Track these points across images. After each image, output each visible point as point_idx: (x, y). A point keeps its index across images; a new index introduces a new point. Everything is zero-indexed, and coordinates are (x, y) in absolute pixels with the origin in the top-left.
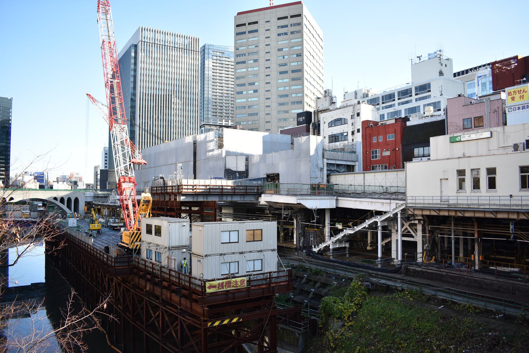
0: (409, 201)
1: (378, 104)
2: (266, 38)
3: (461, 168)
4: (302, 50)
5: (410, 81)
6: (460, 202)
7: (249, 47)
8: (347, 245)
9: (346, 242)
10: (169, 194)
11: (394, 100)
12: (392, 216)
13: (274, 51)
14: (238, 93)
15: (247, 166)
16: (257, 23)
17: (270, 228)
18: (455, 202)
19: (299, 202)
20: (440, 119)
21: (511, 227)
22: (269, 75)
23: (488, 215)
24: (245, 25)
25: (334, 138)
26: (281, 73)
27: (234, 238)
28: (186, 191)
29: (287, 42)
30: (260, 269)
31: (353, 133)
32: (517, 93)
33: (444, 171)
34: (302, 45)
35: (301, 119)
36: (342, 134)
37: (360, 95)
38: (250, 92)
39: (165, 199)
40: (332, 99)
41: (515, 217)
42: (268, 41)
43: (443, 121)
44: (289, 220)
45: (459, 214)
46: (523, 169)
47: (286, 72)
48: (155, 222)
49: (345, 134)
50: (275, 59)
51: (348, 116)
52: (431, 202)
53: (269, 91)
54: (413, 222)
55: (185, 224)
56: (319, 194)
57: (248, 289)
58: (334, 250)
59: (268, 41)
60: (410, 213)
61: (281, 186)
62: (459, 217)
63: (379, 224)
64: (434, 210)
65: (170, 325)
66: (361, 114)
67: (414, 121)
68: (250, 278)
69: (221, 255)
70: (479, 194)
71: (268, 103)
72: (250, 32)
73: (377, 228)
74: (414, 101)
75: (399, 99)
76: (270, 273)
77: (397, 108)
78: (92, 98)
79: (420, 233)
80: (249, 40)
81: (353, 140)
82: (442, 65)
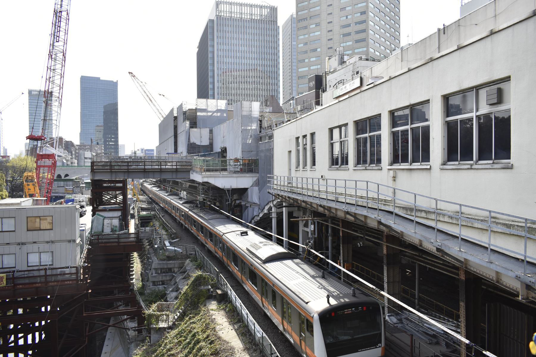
4: (367, 6)
7: (311, 10)
15: (211, 139)
19: (206, 180)
22: (331, 39)
26: (345, 35)
28: (150, 167)
30: (50, 263)
35: (313, 84)
38: (312, 59)
40: (342, 58)
68: (13, 275)
69: (19, 244)
78: (134, 76)
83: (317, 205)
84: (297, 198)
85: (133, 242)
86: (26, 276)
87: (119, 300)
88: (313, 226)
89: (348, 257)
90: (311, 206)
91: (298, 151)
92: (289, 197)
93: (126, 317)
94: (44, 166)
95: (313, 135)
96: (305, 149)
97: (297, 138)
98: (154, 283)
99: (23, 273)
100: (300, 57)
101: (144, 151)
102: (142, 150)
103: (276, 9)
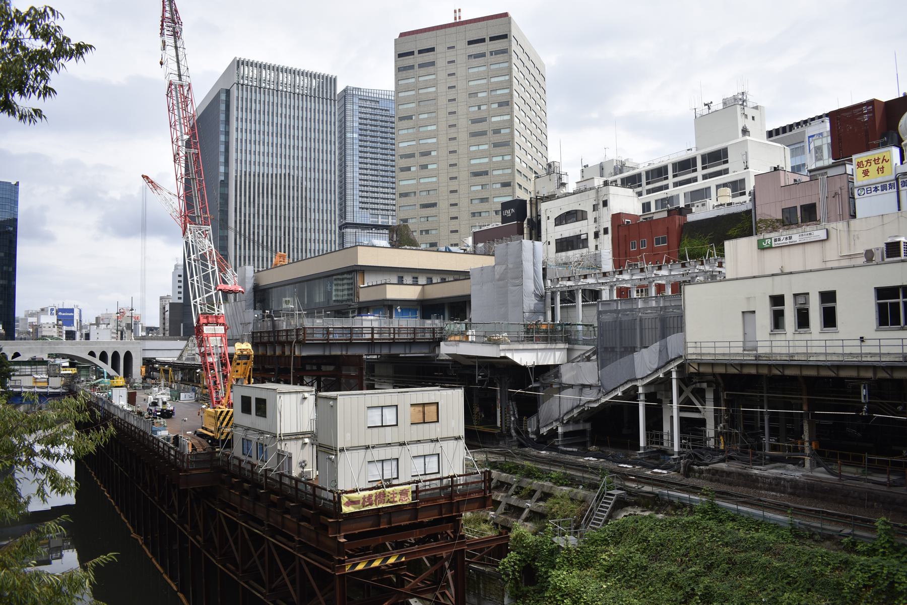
0: (690, 351)
1: (640, 186)
2: (449, 75)
3: (777, 292)
4: (511, 95)
5: (693, 145)
6: (775, 350)
7: (421, 91)
8: (588, 426)
9: (585, 421)
10: (282, 344)
11: (667, 178)
12: (661, 376)
13: (462, 97)
14: (403, 170)
16: (432, 50)
17: (451, 401)
18: (767, 350)
19: (502, 354)
20: (743, 208)
21: (864, 392)
22: (455, 139)
23: (825, 373)
24: (412, 53)
25: (564, 245)
26: (474, 135)
27: (390, 417)
29: (484, 81)
31: (596, 235)
32: (873, 163)
33: (748, 299)
34: (509, 85)
35: (508, 213)
36: (578, 237)
37: (609, 170)
39: (275, 352)
40: (560, 178)
41: (869, 374)
42: (452, 81)
43: (748, 212)
44: (488, 385)
45: (776, 372)
46: (882, 293)
47: (483, 133)
48: (255, 391)
49: (583, 237)
50: (465, 111)
51: (588, 208)
52: (727, 351)
53: (455, 165)
54: (698, 385)
55: (306, 395)
56: (538, 340)
57: (413, 509)
58: (565, 434)
59: (452, 81)
60: (692, 370)
62: (775, 376)
63: (641, 390)
64: (731, 365)
65: (282, 570)
66: (611, 203)
67: (698, 214)
68: (417, 487)
69: (367, 447)
70: (807, 337)
71: (454, 185)
72: (421, 66)
73: (636, 397)
74: (700, 178)
75: (674, 176)
76: (452, 477)
77: (672, 191)
78: (152, 182)
79: (710, 407)
80: (421, 79)
81: (597, 246)
82: (746, 116)
86: (427, 487)
94: (215, 335)
100: (404, 163)
102: (52, 310)
103: (335, 79)
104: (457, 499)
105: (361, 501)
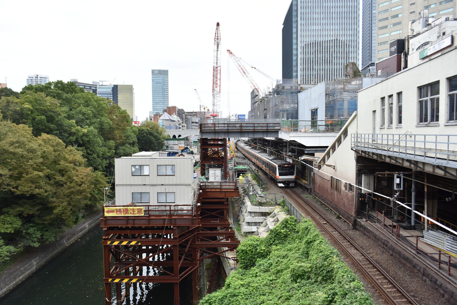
19: (292, 139)
61: (300, 124)
83: (403, 159)
84: (382, 153)
85: (232, 189)
86: (157, 209)
87: (221, 234)
88: (398, 180)
89: (432, 212)
90: (397, 161)
91: (383, 110)
92: (373, 153)
93: (227, 249)
95: (399, 94)
96: (391, 109)
97: (383, 99)
98: (249, 224)
99: (155, 207)
101: (237, 116)
102: (236, 115)
104: (174, 217)
105: (115, 211)
